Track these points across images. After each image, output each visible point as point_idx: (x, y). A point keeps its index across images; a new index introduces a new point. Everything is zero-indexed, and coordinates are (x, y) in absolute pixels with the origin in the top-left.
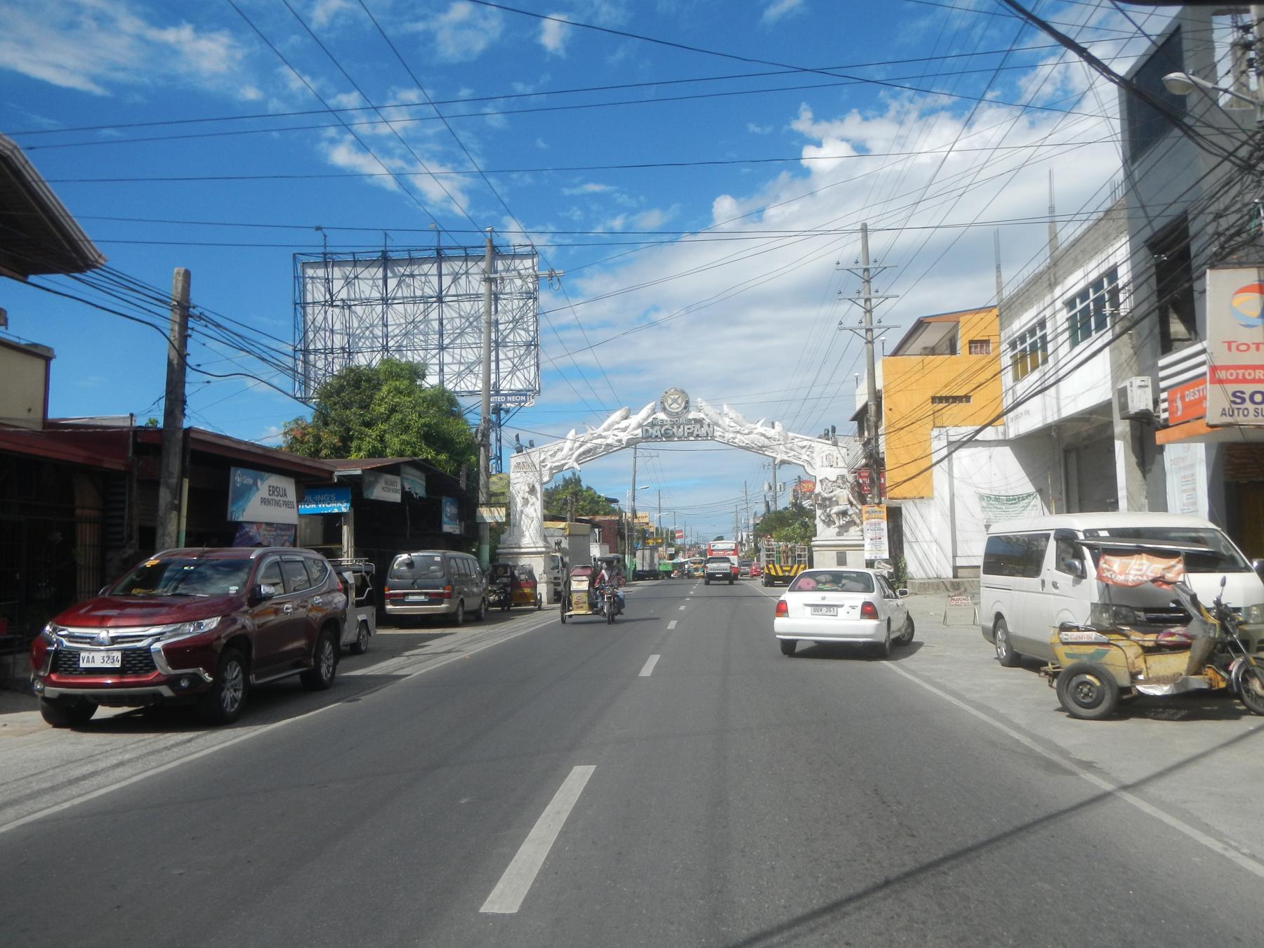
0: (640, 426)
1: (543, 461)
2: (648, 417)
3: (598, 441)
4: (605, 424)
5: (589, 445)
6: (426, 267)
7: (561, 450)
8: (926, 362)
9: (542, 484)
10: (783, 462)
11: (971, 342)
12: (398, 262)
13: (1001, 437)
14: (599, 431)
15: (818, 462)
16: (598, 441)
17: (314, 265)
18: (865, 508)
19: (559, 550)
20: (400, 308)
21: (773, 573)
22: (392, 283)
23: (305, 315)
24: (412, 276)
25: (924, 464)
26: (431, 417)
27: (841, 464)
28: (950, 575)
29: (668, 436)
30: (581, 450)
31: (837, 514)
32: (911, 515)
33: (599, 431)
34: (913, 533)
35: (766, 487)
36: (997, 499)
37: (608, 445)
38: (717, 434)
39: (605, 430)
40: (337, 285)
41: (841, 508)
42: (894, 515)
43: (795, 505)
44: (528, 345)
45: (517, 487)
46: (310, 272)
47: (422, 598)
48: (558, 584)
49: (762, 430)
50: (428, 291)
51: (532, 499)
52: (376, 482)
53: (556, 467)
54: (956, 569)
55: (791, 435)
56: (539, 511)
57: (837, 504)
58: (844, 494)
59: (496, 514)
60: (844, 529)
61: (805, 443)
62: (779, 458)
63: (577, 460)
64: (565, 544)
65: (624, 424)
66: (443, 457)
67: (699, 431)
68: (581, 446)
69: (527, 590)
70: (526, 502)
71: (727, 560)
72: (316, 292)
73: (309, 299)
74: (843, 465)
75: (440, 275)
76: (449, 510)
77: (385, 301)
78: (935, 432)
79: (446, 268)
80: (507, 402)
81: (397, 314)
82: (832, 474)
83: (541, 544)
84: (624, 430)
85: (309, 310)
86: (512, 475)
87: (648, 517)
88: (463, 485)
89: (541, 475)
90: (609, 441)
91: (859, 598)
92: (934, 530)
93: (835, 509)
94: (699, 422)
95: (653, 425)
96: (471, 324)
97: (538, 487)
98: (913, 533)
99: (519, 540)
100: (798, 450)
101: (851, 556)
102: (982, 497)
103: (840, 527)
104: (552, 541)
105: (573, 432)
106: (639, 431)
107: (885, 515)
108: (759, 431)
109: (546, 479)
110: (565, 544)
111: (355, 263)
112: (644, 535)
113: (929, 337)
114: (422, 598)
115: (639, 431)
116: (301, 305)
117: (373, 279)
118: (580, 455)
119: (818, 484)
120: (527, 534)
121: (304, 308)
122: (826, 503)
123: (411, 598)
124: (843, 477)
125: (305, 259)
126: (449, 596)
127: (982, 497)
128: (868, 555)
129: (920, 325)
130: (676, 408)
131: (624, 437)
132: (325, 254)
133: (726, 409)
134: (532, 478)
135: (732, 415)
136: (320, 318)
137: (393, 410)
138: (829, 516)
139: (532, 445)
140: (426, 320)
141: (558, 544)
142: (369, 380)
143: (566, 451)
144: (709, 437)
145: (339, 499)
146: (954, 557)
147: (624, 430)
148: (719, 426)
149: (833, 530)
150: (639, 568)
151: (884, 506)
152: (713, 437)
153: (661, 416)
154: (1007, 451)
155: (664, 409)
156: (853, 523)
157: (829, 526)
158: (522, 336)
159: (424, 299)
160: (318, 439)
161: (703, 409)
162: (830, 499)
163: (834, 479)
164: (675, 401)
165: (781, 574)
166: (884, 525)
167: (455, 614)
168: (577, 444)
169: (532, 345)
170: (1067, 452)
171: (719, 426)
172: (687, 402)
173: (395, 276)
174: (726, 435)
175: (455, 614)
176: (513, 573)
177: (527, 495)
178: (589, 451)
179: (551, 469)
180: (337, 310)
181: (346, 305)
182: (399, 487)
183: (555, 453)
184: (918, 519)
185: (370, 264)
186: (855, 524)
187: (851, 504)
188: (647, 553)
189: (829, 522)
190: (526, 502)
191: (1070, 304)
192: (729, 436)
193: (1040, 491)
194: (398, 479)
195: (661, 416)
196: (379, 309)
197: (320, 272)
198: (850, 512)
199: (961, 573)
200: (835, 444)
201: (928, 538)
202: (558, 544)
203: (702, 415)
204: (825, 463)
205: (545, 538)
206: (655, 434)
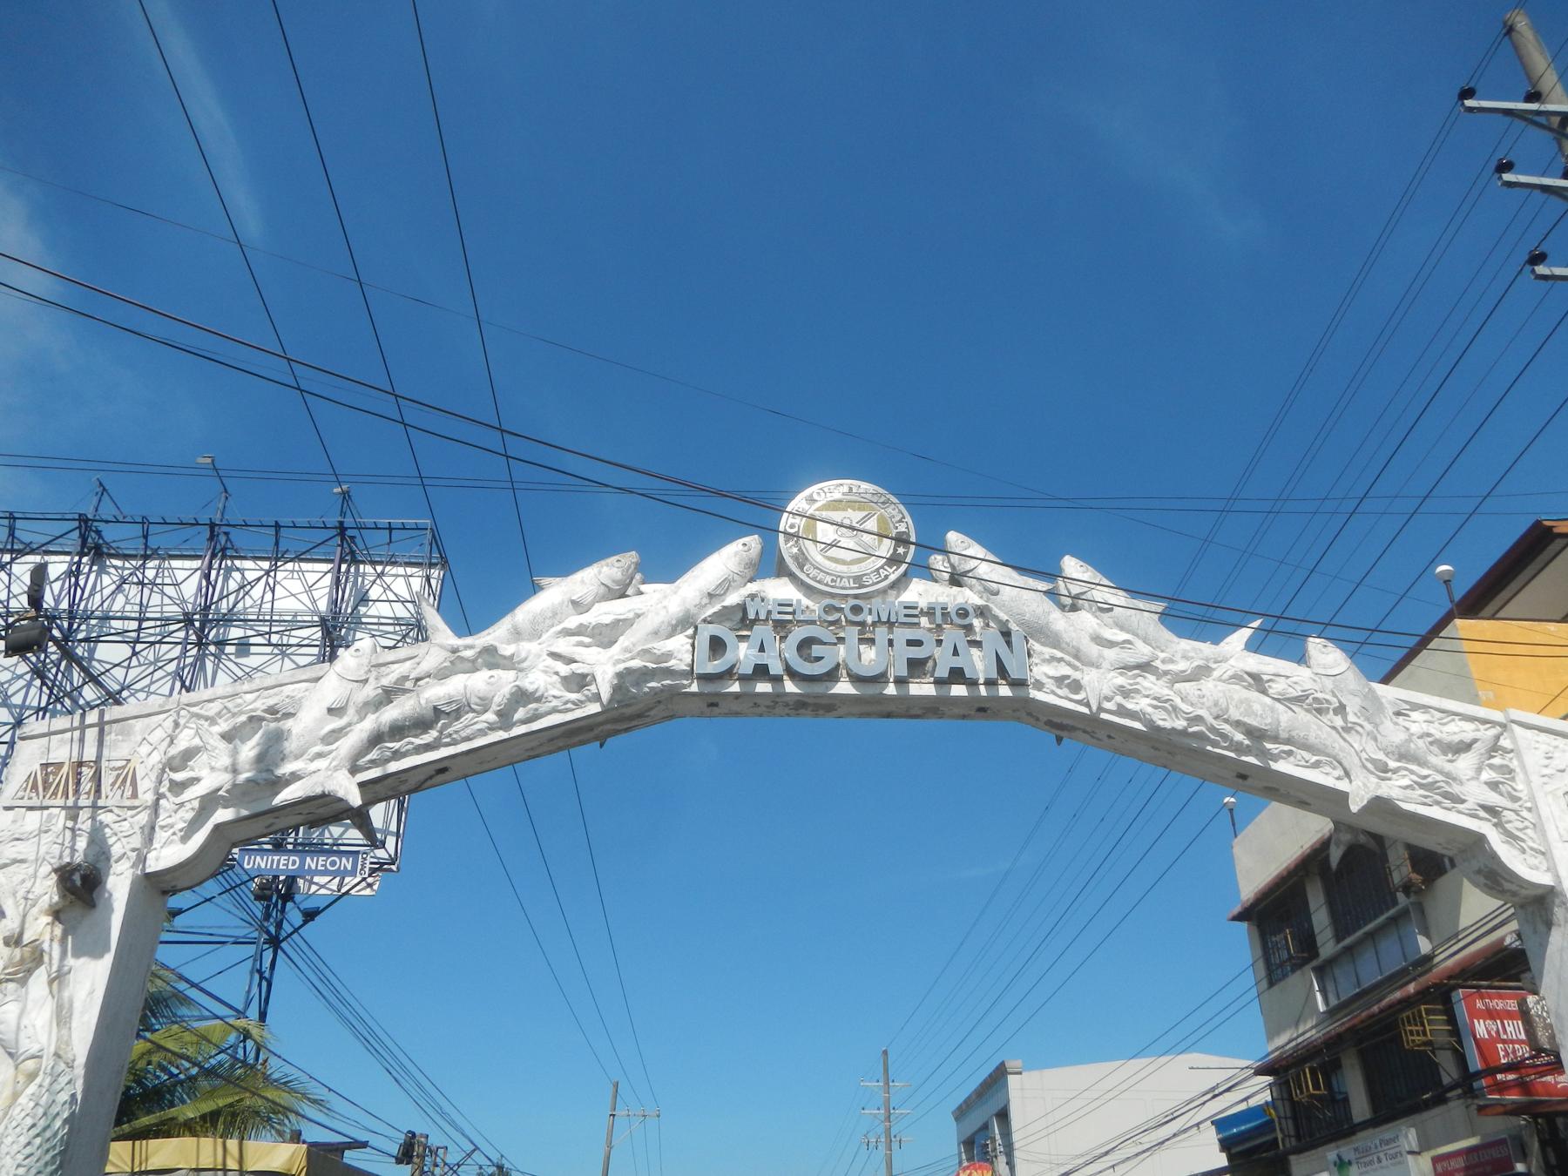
0: (686, 622)
2: (726, 585)
3: (477, 682)
16: (477, 682)
30: (391, 714)
33: (496, 635)
37: (522, 696)
68: (388, 695)
84: (605, 636)
90: (535, 680)
95: (742, 618)
100: (1438, 760)
118: (376, 739)
147: (605, 636)
168: (370, 691)
171: (1054, 641)
174: (1089, 677)
178: (421, 724)
203: (969, 596)
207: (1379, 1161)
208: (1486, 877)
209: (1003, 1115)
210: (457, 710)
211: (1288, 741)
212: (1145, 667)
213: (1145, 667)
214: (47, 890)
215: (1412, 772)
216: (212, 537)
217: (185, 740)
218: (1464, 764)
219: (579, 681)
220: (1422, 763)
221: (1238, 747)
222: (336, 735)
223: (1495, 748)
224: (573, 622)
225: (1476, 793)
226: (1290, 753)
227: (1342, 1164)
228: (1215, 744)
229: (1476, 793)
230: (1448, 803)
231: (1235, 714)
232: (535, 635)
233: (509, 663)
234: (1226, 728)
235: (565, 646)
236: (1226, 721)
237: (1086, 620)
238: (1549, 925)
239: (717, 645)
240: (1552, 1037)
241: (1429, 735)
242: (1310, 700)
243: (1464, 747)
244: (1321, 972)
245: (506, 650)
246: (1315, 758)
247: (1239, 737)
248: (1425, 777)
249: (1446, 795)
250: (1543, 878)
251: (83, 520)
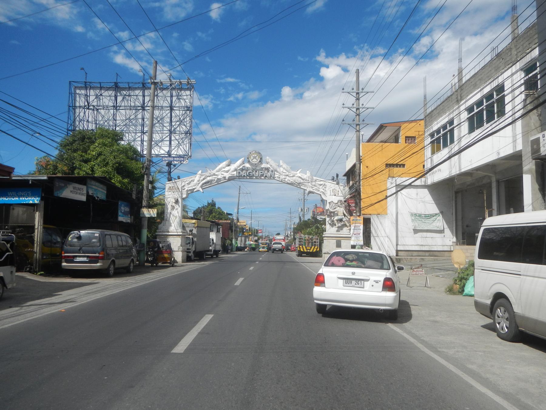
0: (236, 170)
1: (184, 186)
2: (240, 165)
4: (218, 168)
5: (209, 179)
6: (137, 92)
7: (193, 181)
8: (384, 146)
9: (183, 199)
10: (310, 192)
11: (406, 137)
12: (124, 89)
13: (423, 184)
14: (214, 171)
15: (328, 193)
17: (80, 88)
18: (352, 218)
19: (192, 234)
20: (123, 112)
21: (302, 250)
22: (120, 99)
23: (75, 113)
24: (129, 96)
25: (381, 196)
26: (122, 158)
27: (340, 194)
28: (395, 254)
29: (250, 176)
30: (204, 181)
31: (337, 220)
32: (375, 222)
33: (214, 171)
34: (376, 232)
35: (300, 209)
36: (420, 216)
37: (218, 179)
38: (276, 176)
39: (217, 171)
40: (92, 98)
41: (340, 217)
42: (367, 222)
43: (313, 218)
44: (186, 133)
45: (169, 199)
46: (78, 91)
47: (85, 259)
48: (190, 252)
49: (299, 175)
50: (138, 104)
51: (176, 206)
52: (65, 187)
53: (190, 190)
54: (397, 251)
55: (315, 178)
56: (180, 213)
57: (337, 215)
58: (341, 210)
59: (151, 212)
60: (340, 228)
61: (322, 183)
62: (309, 189)
63: (201, 187)
64: (195, 231)
65: (227, 168)
66: (126, 180)
67: (267, 175)
68: (204, 179)
69: (166, 255)
70: (173, 208)
71: (280, 244)
72: (80, 101)
73: (77, 104)
74: (341, 195)
75: (144, 96)
76: (123, 208)
77: (115, 107)
78: (390, 180)
79: (147, 92)
80: (174, 160)
81: (121, 115)
82: (335, 199)
83: (180, 230)
85: (77, 111)
86: (166, 193)
87: (244, 222)
88: (134, 197)
89: (182, 194)
90: (219, 177)
91: (381, 275)
92: (387, 231)
93: (336, 218)
94: (267, 169)
95: (242, 170)
96: (159, 121)
97: (180, 200)
98: (376, 232)
99: (168, 228)
101: (343, 243)
102: (412, 215)
103: (338, 227)
104: (188, 229)
105: (200, 172)
106: (235, 173)
107: (362, 222)
108: (298, 175)
109: (184, 196)
110: (195, 231)
111: (101, 88)
112: (242, 230)
113: (384, 135)
114: (85, 259)
115: (235, 173)
116: (73, 107)
117: (110, 96)
118: (203, 184)
119: (328, 204)
120: (173, 225)
121: (74, 110)
122: (331, 214)
123: (78, 259)
124: (341, 201)
125: (76, 85)
126: (102, 258)
127: (412, 215)
128: (352, 243)
129: (381, 128)
130: (255, 161)
131: (227, 175)
132: (86, 82)
133: (281, 163)
134: (177, 195)
135: (285, 166)
136: (82, 114)
137: (100, 154)
138: (333, 221)
139: (179, 178)
140: (136, 118)
141: (191, 231)
142: (89, 138)
143: (196, 181)
144: (272, 177)
145: (33, 195)
146: (397, 245)
147: (227, 172)
148: (278, 172)
149: (335, 229)
150: (239, 245)
151: (362, 217)
152: (274, 178)
153: (247, 165)
154: (426, 191)
155: (249, 162)
156: (345, 225)
157: (332, 226)
158: (184, 128)
159: (135, 108)
160: (56, 167)
161: (269, 163)
162: (334, 212)
164: (255, 158)
165: (305, 251)
166: (362, 227)
167: (108, 269)
168: (202, 178)
169: (188, 133)
170: (456, 193)
172: (261, 159)
173: (121, 95)
175: (108, 269)
176: (159, 246)
177: (174, 204)
178: (208, 182)
179: (187, 191)
180: (91, 111)
181: (96, 109)
182: (85, 192)
183: (190, 182)
184: (379, 225)
185: (108, 89)
186: (346, 226)
187: (345, 215)
188: (243, 238)
189: (333, 224)
190: (173, 208)
191: (470, 109)
192: (282, 177)
193: (442, 212)
194: (84, 188)
195: (247, 165)
196: (112, 111)
197: (83, 92)
198: (344, 220)
199: (400, 253)
200: (338, 184)
201: (384, 234)
202: (191, 231)
203: (269, 166)
204: (332, 194)
205: (183, 227)
206: (243, 176)
210: (212, 181)
212: (287, 175)
213: (287, 175)
214: (174, 201)
216: (143, 85)
217: (183, 185)
218: (321, 187)
219: (225, 178)
222: (199, 184)
224: (223, 170)
225: (321, 190)
232: (219, 171)
233: (217, 175)
235: (223, 173)
237: (282, 169)
239: (239, 173)
243: (321, 185)
245: (216, 173)
251: (115, 83)
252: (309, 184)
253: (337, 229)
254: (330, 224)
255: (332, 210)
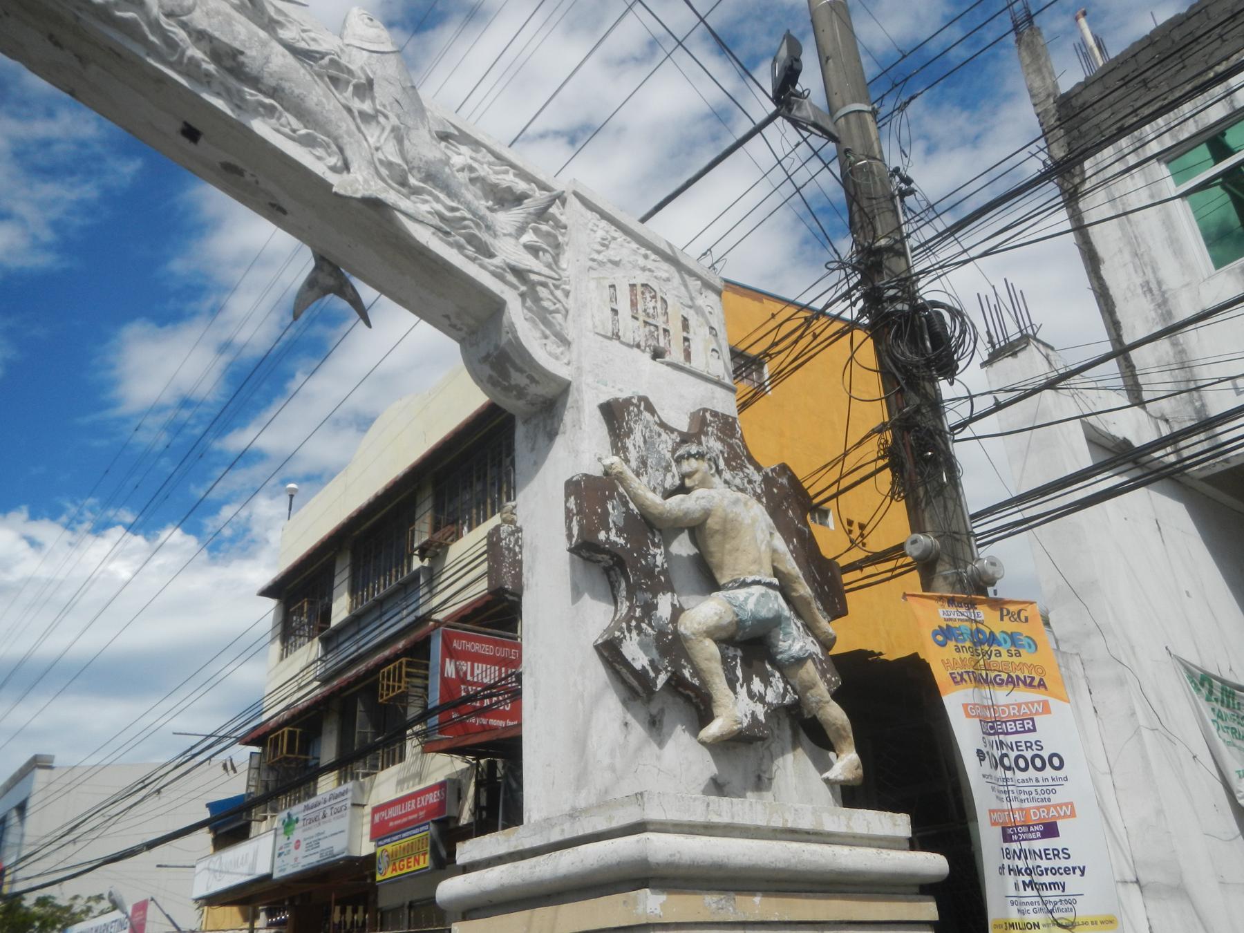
41: (757, 601)
93: (704, 613)
103: (734, 746)
124: (727, 427)
138: (672, 646)
163: (683, 425)
189: (663, 693)
198: (794, 642)
204: (631, 329)
207: (325, 816)
208: (493, 366)
209: (21, 808)
211: (274, 92)
215: (437, 200)
218: (506, 219)
220: (451, 194)
221: (191, 69)
223: (542, 214)
225: (510, 251)
226: (270, 111)
227: (289, 824)
228: (152, 50)
229: (510, 251)
230: (470, 250)
231: (199, 20)
234: (180, 35)
236: (184, 26)
238: (552, 435)
240: (519, 576)
241: (471, 169)
242: (327, 59)
244: (331, 640)
246: (303, 131)
247: (194, 52)
248: (453, 209)
249: (472, 239)
250: (560, 370)
252: (373, 135)
253: (705, 766)
254: (634, 688)
255: (654, 499)
